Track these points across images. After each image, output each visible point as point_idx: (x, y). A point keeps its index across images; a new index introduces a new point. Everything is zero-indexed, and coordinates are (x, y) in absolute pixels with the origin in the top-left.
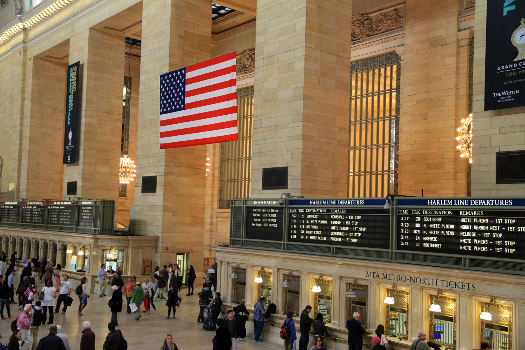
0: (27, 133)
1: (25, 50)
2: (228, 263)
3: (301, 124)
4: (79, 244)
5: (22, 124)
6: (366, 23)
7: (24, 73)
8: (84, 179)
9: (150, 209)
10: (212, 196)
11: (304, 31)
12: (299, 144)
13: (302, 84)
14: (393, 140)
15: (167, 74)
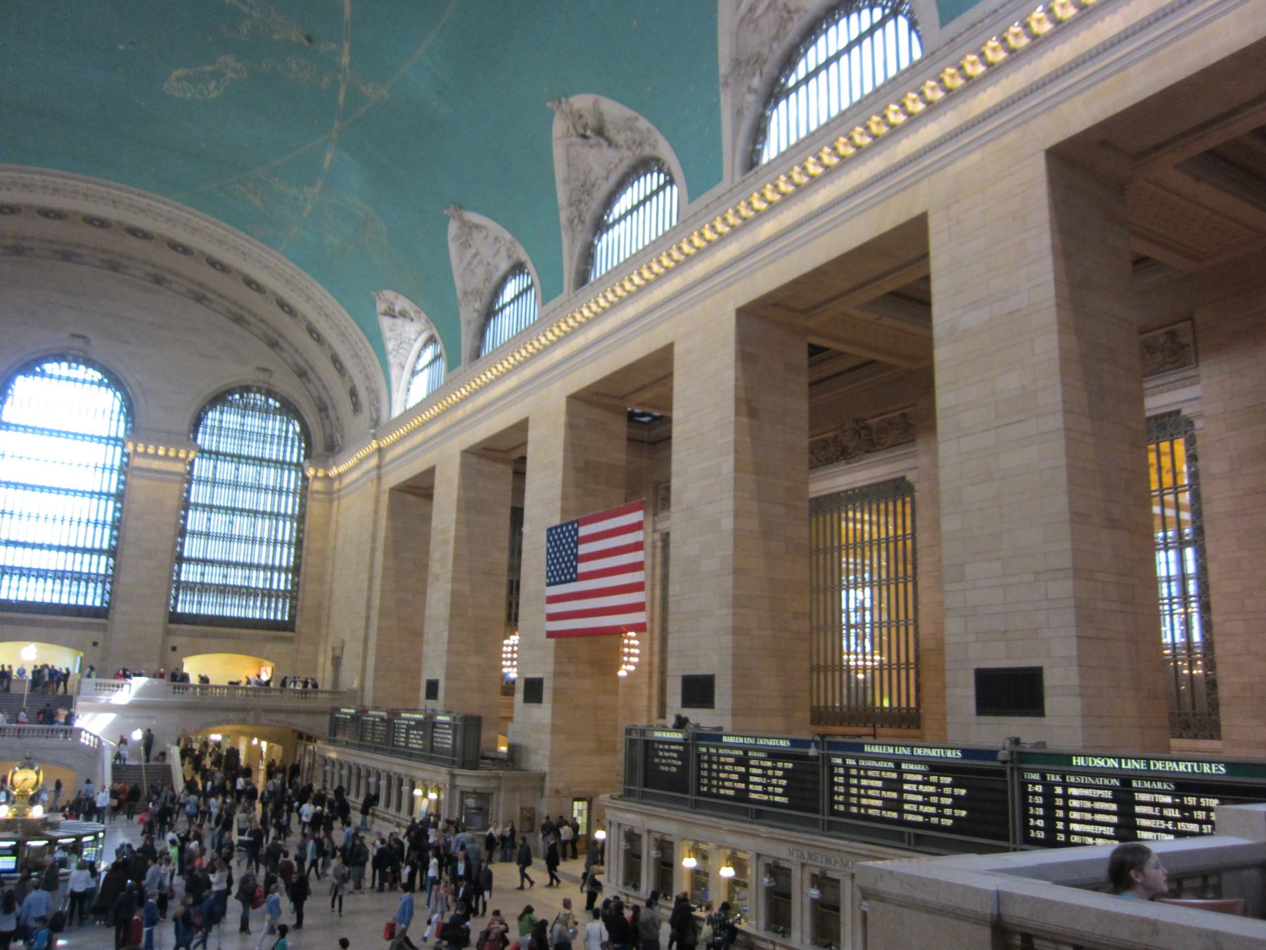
0: (376, 602)
1: (379, 478)
2: (619, 825)
3: (730, 611)
4: (431, 781)
5: (370, 588)
6: (863, 432)
7: (376, 512)
8: (447, 677)
9: (532, 727)
10: (650, 698)
11: (732, 475)
12: (728, 640)
13: (730, 552)
14: (911, 616)
15: (556, 528)
